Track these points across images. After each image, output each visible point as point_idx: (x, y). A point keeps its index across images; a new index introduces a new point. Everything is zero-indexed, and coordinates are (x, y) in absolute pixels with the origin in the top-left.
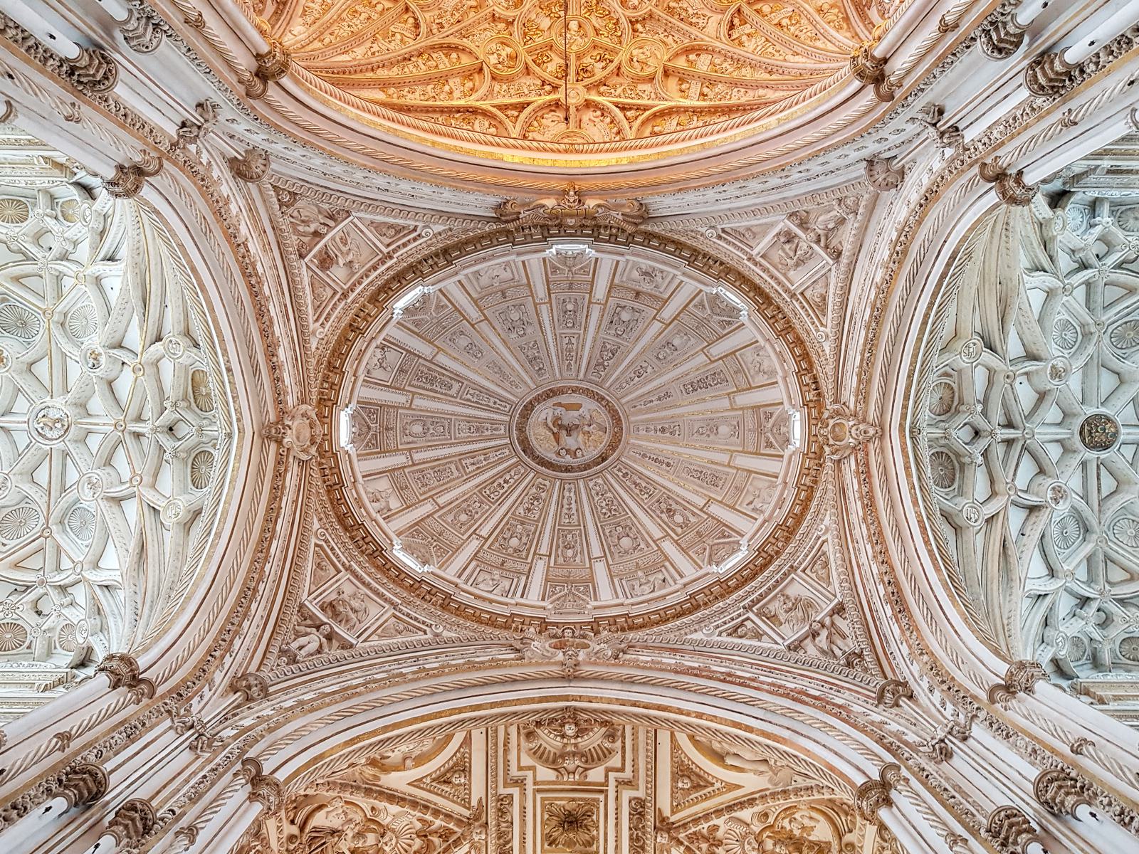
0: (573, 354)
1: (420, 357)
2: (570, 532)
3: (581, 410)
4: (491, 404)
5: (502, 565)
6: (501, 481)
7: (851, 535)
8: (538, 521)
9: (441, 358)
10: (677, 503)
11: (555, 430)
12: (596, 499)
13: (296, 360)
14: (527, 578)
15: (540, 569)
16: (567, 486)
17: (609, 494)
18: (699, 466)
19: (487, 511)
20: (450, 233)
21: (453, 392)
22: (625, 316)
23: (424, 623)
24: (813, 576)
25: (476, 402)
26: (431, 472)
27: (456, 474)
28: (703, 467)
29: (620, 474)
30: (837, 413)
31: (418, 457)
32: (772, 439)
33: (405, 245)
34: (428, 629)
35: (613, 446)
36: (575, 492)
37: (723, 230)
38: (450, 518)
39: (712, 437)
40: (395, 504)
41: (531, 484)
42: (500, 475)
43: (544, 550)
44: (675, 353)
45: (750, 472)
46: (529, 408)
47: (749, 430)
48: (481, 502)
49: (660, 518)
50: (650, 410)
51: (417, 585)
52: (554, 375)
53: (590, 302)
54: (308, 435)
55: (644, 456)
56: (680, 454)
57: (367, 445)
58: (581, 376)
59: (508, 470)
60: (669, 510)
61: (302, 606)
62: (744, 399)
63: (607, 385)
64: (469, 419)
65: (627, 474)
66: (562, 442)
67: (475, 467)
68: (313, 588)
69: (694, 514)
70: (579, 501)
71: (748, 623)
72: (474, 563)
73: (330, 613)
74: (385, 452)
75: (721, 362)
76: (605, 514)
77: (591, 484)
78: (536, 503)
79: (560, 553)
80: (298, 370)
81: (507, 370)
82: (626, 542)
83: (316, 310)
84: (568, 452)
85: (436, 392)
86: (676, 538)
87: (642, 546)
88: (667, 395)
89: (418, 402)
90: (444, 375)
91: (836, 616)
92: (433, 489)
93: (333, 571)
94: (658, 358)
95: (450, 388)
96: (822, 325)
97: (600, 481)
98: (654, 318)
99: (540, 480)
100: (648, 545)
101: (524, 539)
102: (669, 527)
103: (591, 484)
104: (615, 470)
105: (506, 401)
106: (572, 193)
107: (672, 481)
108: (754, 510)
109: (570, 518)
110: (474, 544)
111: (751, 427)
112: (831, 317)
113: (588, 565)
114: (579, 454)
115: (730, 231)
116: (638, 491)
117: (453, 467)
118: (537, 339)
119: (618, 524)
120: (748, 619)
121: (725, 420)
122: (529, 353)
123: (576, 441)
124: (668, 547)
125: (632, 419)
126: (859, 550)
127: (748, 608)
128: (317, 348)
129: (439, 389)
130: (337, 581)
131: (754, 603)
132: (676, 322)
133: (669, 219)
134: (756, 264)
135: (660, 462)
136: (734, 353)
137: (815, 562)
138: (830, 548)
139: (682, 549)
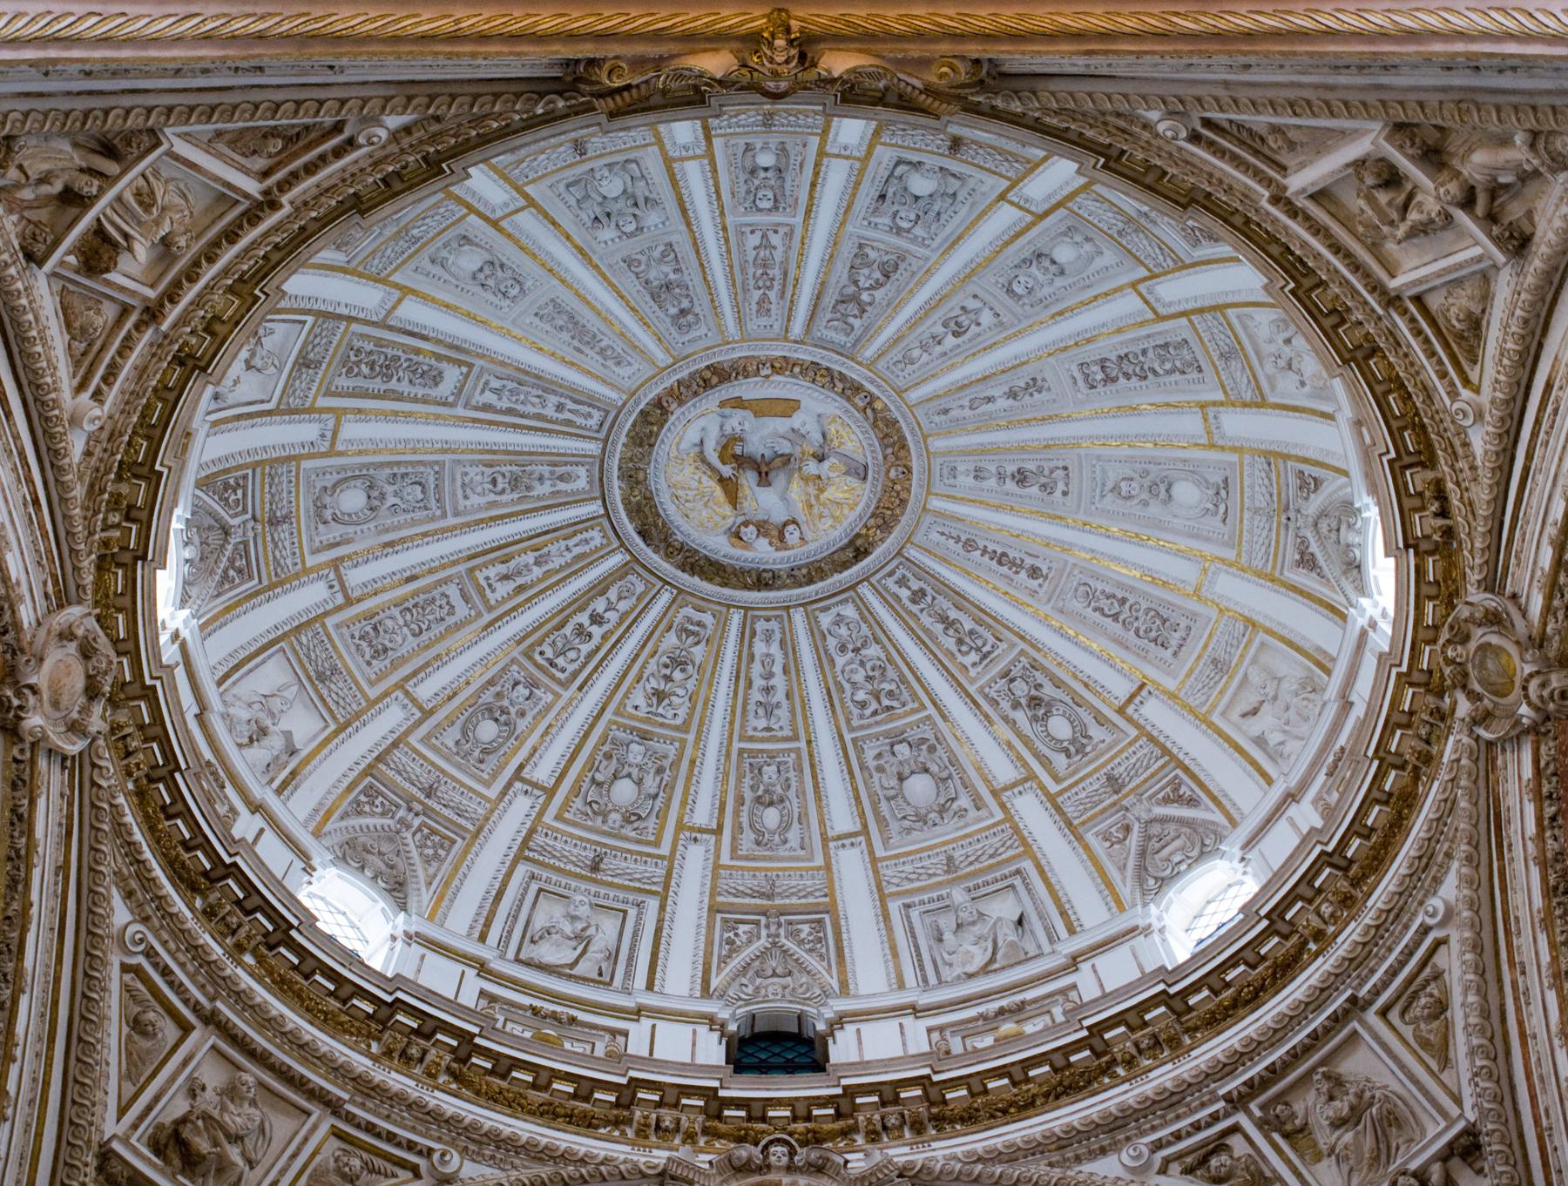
0: (776, 272)
1: (351, 319)
2: (772, 755)
3: (797, 421)
4: (550, 411)
5: (595, 867)
6: (583, 618)
7: (1509, 944)
8: (685, 727)
9: (412, 312)
10: (1058, 683)
11: (727, 471)
12: (840, 661)
13: (36, 502)
14: (662, 908)
15: (694, 865)
16: (760, 626)
17: (873, 651)
18: (1120, 585)
19: (548, 708)
20: (435, 128)
21: (445, 389)
22: (921, 185)
23: (411, 1146)
24: (1408, 1032)
25: (510, 411)
26: (396, 612)
27: (462, 610)
28: (1132, 589)
29: (904, 593)
30: (1493, 619)
31: (356, 577)
32: (1314, 548)
33: (310, 169)
34: (421, 1162)
35: (884, 517)
36: (782, 643)
37: (1207, 123)
38: (451, 737)
39: (1155, 509)
40: (303, 725)
41: (664, 624)
42: (580, 602)
43: (703, 815)
44: (1060, 282)
45: (1251, 624)
46: (654, 418)
47: (1256, 511)
48: (533, 684)
49: (1012, 723)
50: (984, 425)
51: (385, 1011)
52: (721, 329)
53: (822, 153)
54: (80, 684)
55: (969, 545)
56: (1067, 548)
57: (225, 577)
58: (797, 329)
59: (600, 588)
60: (1035, 702)
61: (106, 1155)
62: (1239, 425)
63: (869, 352)
64: (490, 457)
65: (923, 593)
66: (748, 505)
67: (510, 586)
68: (129, 1090)
69: (1101, 720)
70: (792, 668)
71: (1236, 1142)
72: (522, 870)
73: (177, 1162)
74: (279, 583)
75: (1184, 321)
76: (863, 705)
77: (826, 620)
78: (677, 675)
79: (745, 820)
80: (42, 526)
81: (592, 322)
82: (920, 788)
83: (77, 364)
84: (762, 528)
85: (399, 397)
86: (1053, 788)
87: (964, 801)
88: (1034, 385)
89: (353, 430)
90: (418, 351)
91: (1455, 1163)
92: (403, 660)
93: (170, 1031)
94: (1010, 291)
95: (437, 379)
96: (1466, 382)
97: (849, 611)
98: (1002, 197)
99: (689, 611)
100: (978, 804)
101: (651, 783)
102: (1037, 755)
103: (826, 620)
104: (890, 582)
105: (591, 401)
106: (780, 43)
107: (1044, 621)
108: (1260, 741)
109: (769, 714)
110: (520, 809)
111: (1261, 501)
112: (1491, 370)
113: (819, 861)
114: (792, 536)
115: (1226, 125)
116: (950, 643)
117: (453, 591)
118: (674, 238)
119: (896, 738)
120: (1235, 1129)
121: (1193, 472)
122: (652, 275)
123: (784, 498)
124: (1031, 812)
125: (937, 444)
126: (1526, 992)
127: (1237, 1102)
128: (88, 453)
129: (404, 387)
130: (185, 1063)
131: (1254, 1088)
132: (1062, 212)
133: (1053, 85)
134: (1293, 212)
135: (1013, 563)
136: (1220, 308)
137: (1415, 996)
138: (1455, 963)
139: (1069, 824)
